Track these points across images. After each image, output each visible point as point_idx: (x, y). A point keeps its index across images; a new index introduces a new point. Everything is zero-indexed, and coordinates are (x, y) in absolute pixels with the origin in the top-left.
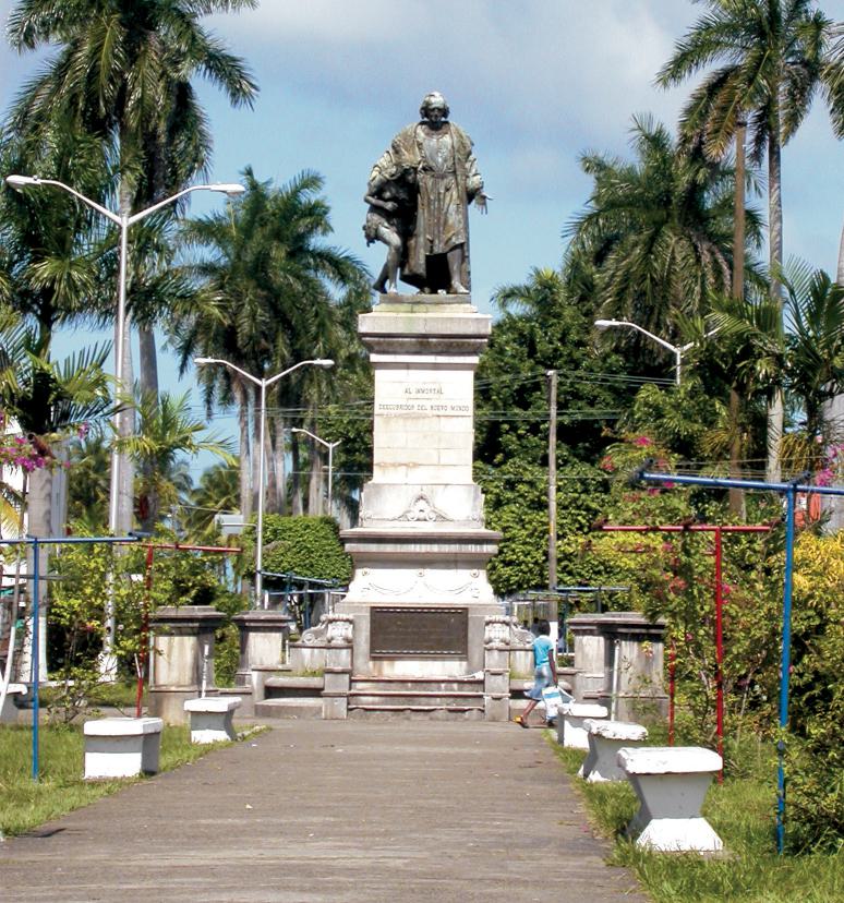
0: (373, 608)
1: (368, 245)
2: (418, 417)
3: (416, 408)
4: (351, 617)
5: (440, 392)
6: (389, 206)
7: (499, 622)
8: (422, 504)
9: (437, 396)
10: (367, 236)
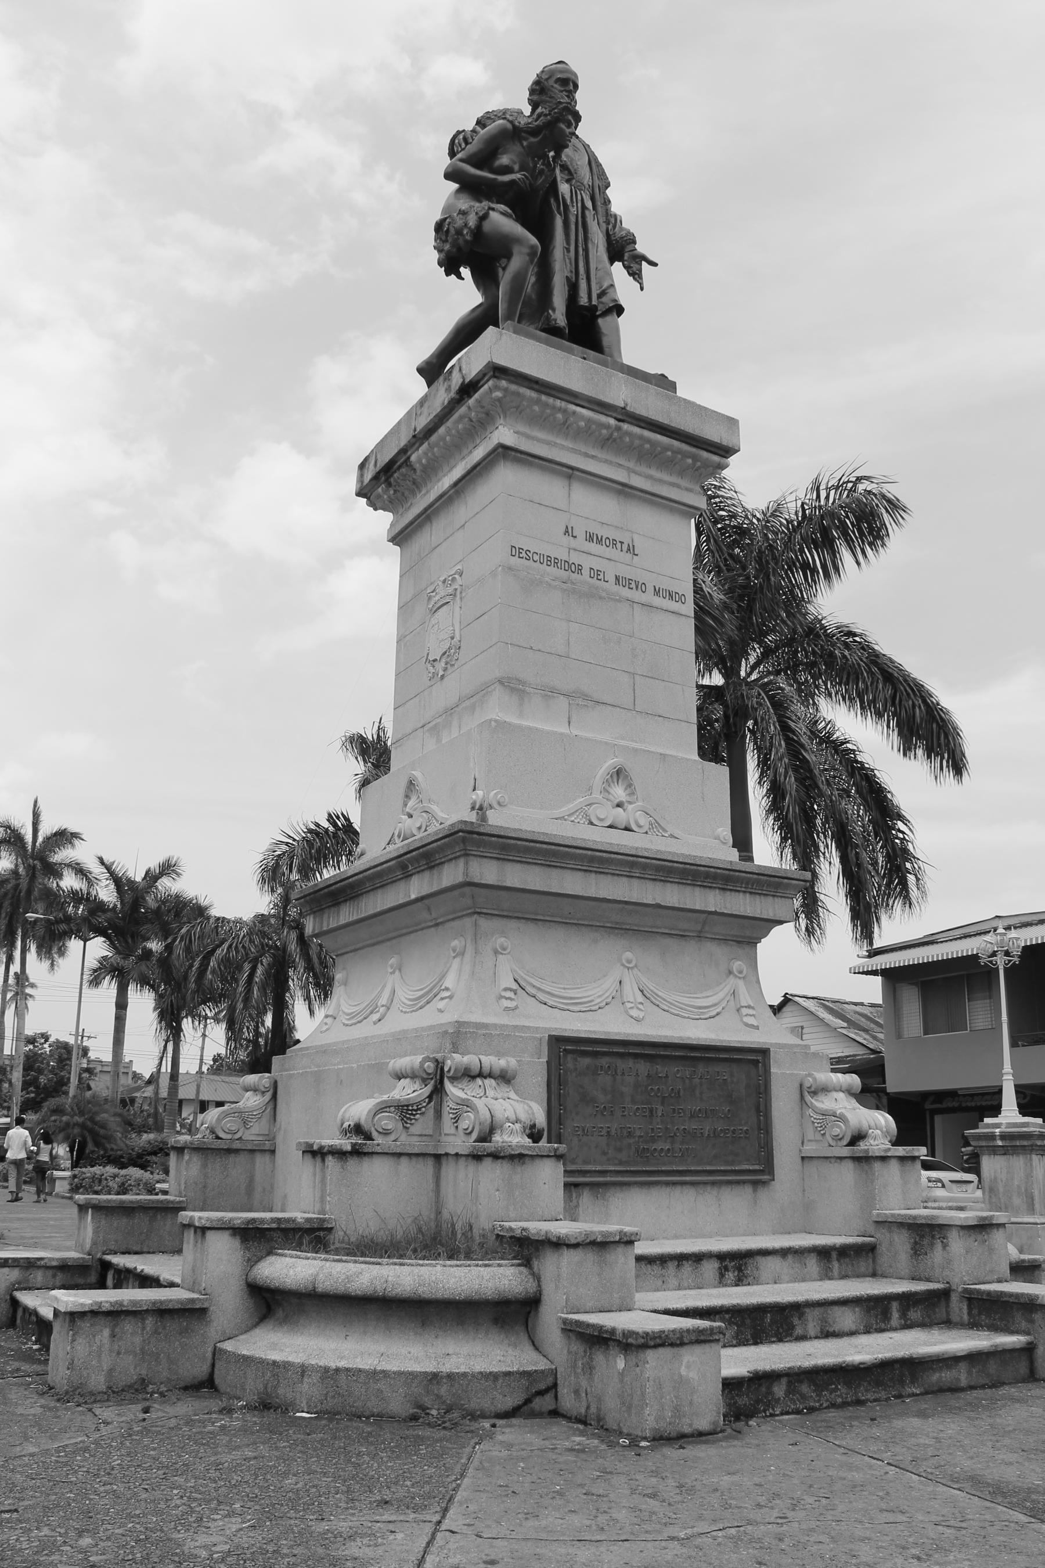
2: (591, 595)
3: (586, 572)
5: (631, 550)
8: (619, 792)
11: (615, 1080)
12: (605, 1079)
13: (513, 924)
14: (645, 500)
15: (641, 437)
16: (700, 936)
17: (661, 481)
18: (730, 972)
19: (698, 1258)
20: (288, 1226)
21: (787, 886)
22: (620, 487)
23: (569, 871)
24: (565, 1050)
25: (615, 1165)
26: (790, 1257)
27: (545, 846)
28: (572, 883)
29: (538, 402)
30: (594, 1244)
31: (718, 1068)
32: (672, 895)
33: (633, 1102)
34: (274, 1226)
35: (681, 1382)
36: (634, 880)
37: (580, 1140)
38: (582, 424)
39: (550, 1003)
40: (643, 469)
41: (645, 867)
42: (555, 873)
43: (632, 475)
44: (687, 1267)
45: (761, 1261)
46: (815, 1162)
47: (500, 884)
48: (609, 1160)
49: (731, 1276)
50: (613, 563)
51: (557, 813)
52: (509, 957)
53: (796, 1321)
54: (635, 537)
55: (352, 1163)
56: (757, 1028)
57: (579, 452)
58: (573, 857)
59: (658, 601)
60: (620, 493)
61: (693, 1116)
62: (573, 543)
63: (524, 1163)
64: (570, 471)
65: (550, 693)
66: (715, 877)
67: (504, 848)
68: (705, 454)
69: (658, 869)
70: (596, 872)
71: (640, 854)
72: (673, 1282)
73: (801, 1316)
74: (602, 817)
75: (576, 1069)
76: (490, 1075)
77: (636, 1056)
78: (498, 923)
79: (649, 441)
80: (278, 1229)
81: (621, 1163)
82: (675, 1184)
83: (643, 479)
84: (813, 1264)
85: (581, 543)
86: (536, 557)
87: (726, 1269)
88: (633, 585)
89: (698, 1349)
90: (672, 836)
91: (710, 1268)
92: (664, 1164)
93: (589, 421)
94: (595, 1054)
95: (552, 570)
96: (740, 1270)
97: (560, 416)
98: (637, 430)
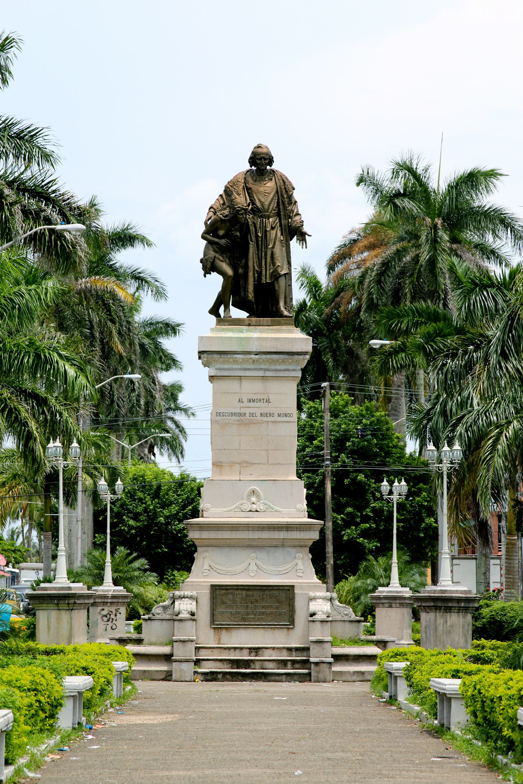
0: (212, 586)
1: (205, 276)
2: (250, 423)
3: (247, 415)
4: (194, 593)
5: (268, 401)
6: (223, 242)
8: (254, 499)
9: (266, 404)
10: (204, 268)
12: (231, 597)
13: (210, 548)
16: (283, 546)
19: (242, 649)
26: (276, 650)
29: (221, 357)
30: (181, 641)
31: (273, 592)
32: (266, 535)
33: (241, 603)
35: (181, 670)
40: (273, 367)
46: (337, 623)
49: (253, 654)
51: (229, 509)
53: (252, 664)
54: (270, 395)
55: (149, 622)
58: (225, 527)
59: (279, 419)
60: (262, 379)
61: (263, 607)
65: (232, 464)
69: (259, 527)
73: (254, 663)
77: (241, 589)
78: (205, 548)
84: (285, 652)
85: (246, 404)
89: (187, 663)
91: (246, 652)
94: (227, 589)
95: (234, 418)
96: (256, 652)
97: (231, 360)
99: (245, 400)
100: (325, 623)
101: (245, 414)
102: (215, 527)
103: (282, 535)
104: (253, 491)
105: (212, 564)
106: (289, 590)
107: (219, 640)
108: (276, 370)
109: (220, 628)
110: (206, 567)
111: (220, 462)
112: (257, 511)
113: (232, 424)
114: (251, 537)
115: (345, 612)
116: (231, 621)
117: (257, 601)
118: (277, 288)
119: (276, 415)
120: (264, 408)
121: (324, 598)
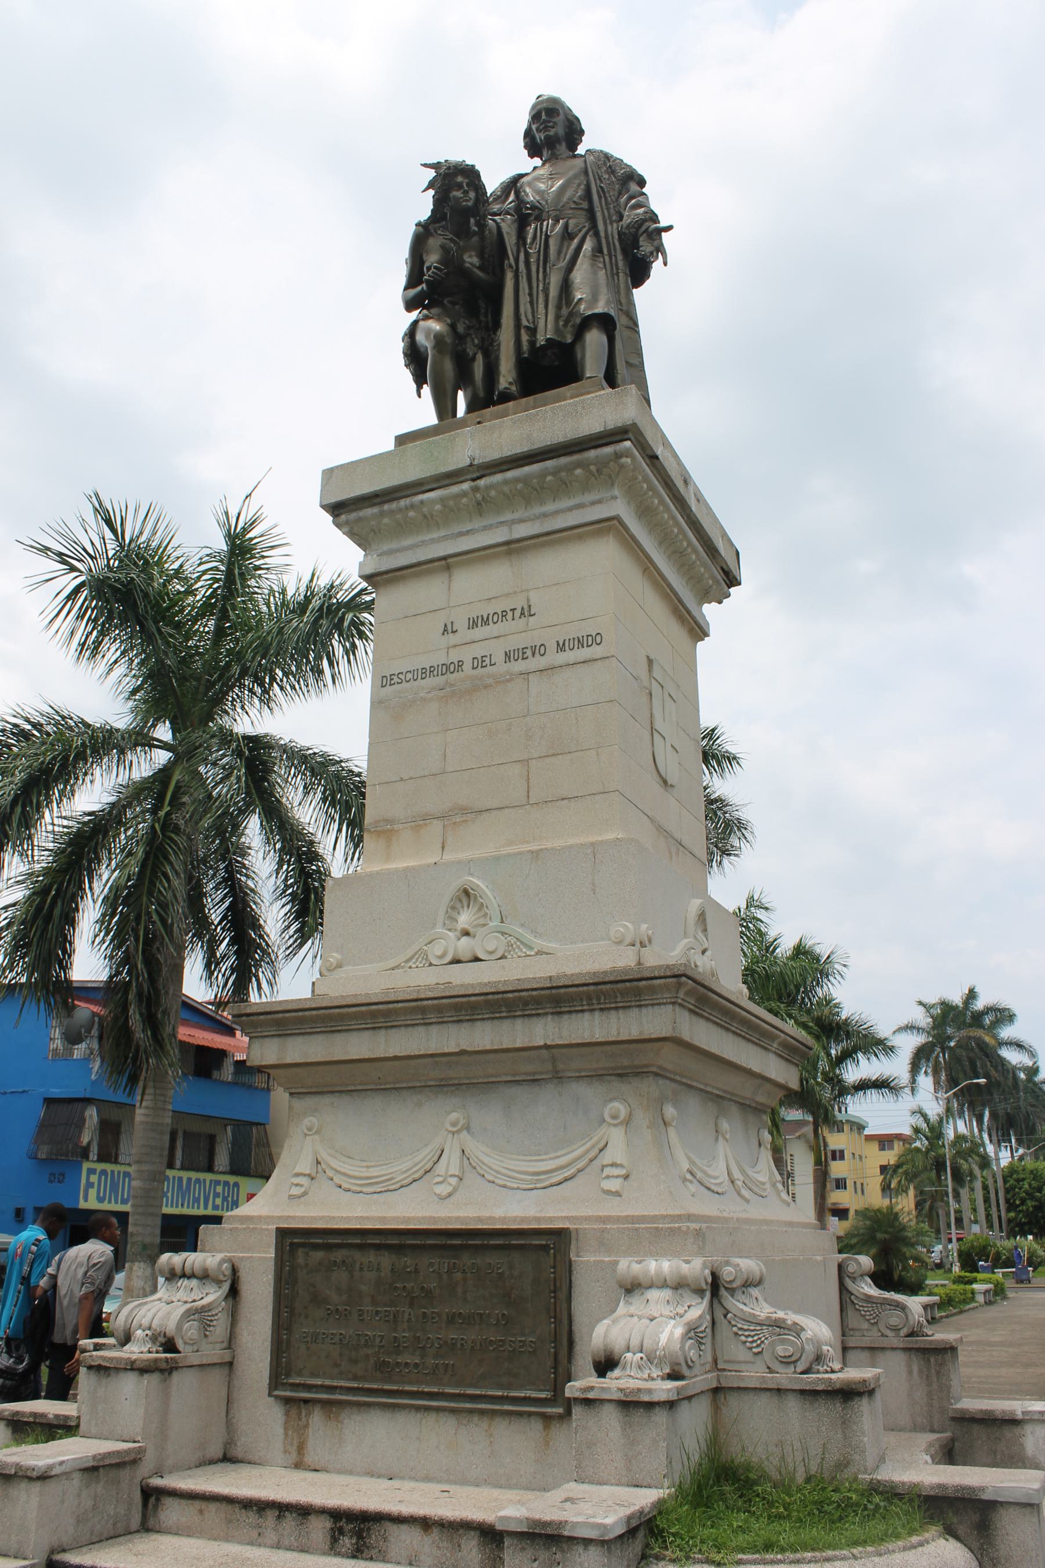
0: (283, 1234)
3: (467, 666)
5: (526, 612)
7: (664, 1285)
8: (465, 918)
11: (352, 1276)
12: (340, 1276)
13: (327, 1100)
14: (543, 545)
15: (506, 482)
16: (558, 1077)
17: (557, 512)
18: (604, 1120)
19: (304, 1511)
20: (42, 1421)
21: (652, 990)
22: (505, 548)
23: (355, 1034)
24: (292, 1244)
25: (348, 1379)
26: (436, 1531)
27: (314, 1012)
28: (358, 1046)
29: (382, 514)
32: (483, 1036)
34: (31, 1419)
36: (431, 1028)
37: (308, 1348)
38: (438, 507)
39: (345, 1185)
41: (439, 1009)
42: (339, 1038)
43: (516, 527)
44: (290, 1521)
45: (392, 1529)
47: (280, 1062)
48: (341, 1373)
49: (347, 1542)
50: (494, 643)
51: (392, 963)
52: (317, 1137)
54: (532, 595)
56: (617, 1194)
57: (445, 538)
60: (509, 553)
61: (451, 1320)
62: (453, 639)
63: (109, 1375)
64: (443, 562)
65: (420, 821)
66: (537, 1002)
67: (279, 1023)
68: (592, 454)
69: (457, 1008)
70: (386, 1028)
71: (422, 996)
72: (271, 1536)
74: (439, 953)
75: (307, 1265)
76: (192, 1276)
77: (378, 1247)
79: (517, 480)
80: (34, 1423)
81: (355, 1378)
82: (427, 1409)
83: (529, 524)
85: (464, 634)
86: (409, 676)
87: (341, 1531)
88: (529, 652)
90: (539, 953)
91: (319, 1527)
92: (411, 1383)
93: (442, 500)
94: (328, 1247)
96: (360, 1537)
97: (411, 514)
98: (498, 478)
99: (461, 624)
100: (639, 1416)
101: (460, 664)
102: (324, 1019)
103: (542, 1031)
104: (466, 892)
105: (324, 1155)
106: (545, 1248)
107: (301, 1449)
108: (545, 515)
109: (306, 1401)
110: (305, 1166)
111: (387, 821)
112: (477, 959)
113: (423, 699)
114: (433, 1047)
115: (781, 1350)
116: (341, 1375)
117: (429, 1293)
118: (579, 356)
119: (552, 646)
120: (515, 634)
121: (679, 1285)
